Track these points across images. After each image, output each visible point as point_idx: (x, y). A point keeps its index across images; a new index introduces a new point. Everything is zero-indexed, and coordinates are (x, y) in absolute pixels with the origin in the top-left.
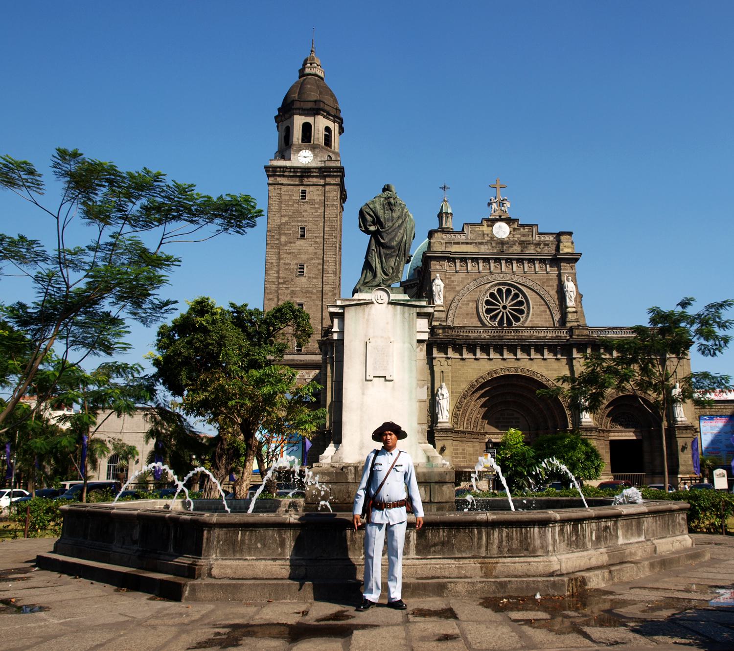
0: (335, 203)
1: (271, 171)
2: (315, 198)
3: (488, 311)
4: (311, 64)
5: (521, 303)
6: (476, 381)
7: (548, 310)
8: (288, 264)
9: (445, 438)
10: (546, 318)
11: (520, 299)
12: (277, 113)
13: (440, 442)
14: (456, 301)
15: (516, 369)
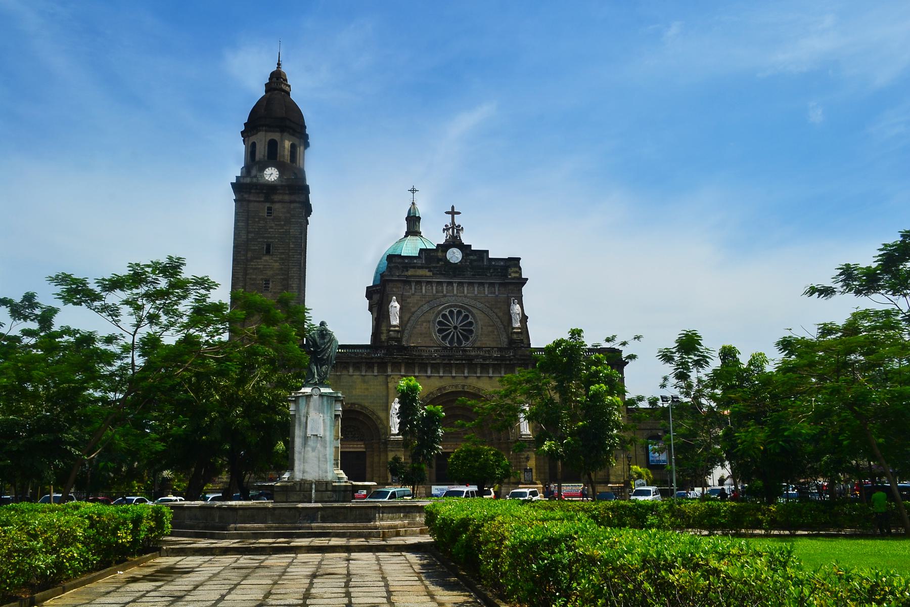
0: (300, 220)
1: (237, 187)
2: (281, 215)
3: (440, 331)
4: (277, 79)
5: (471, 324)
6: (427, 397)
7: (496, 331)
8: (255, 279)
9: (398, 449)
10: (493, 338)
11: (469, 320)
12: (243, 128)
13: (393, 453)
14: (411, 322)
15: (464, 386)
